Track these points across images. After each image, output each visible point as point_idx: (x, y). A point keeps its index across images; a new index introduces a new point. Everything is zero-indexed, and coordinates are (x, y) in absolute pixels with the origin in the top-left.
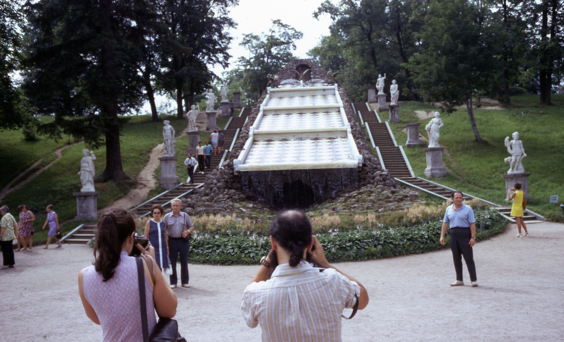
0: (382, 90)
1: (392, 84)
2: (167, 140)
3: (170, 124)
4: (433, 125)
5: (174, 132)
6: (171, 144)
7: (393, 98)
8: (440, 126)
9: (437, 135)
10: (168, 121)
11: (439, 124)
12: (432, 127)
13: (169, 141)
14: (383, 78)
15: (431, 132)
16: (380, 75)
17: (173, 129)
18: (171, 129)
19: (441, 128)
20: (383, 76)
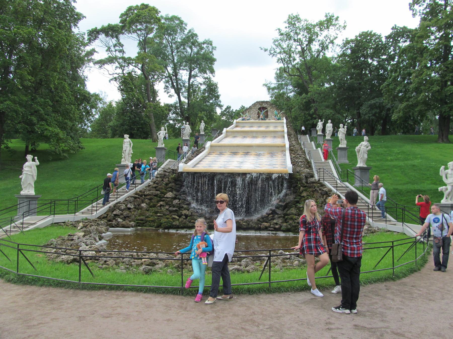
0: (321, 130)
1: (328, 123)
2: (126, 150)
3: (129, 138)
4: (362, 147)
5: (132, 144)
6: (129, 154)
7: (329, 134)
8: (368, 149)
9: (366, 156)
10: (128, 136)
11: (367, 147)
12: (361, 149)
13: (127, 151)
14: (322, 122)
15: (360, 153)
16: (320, 120)
17: (131, 142)
18: (129, 142)
19: (368, 151)
20: (321, 121)
